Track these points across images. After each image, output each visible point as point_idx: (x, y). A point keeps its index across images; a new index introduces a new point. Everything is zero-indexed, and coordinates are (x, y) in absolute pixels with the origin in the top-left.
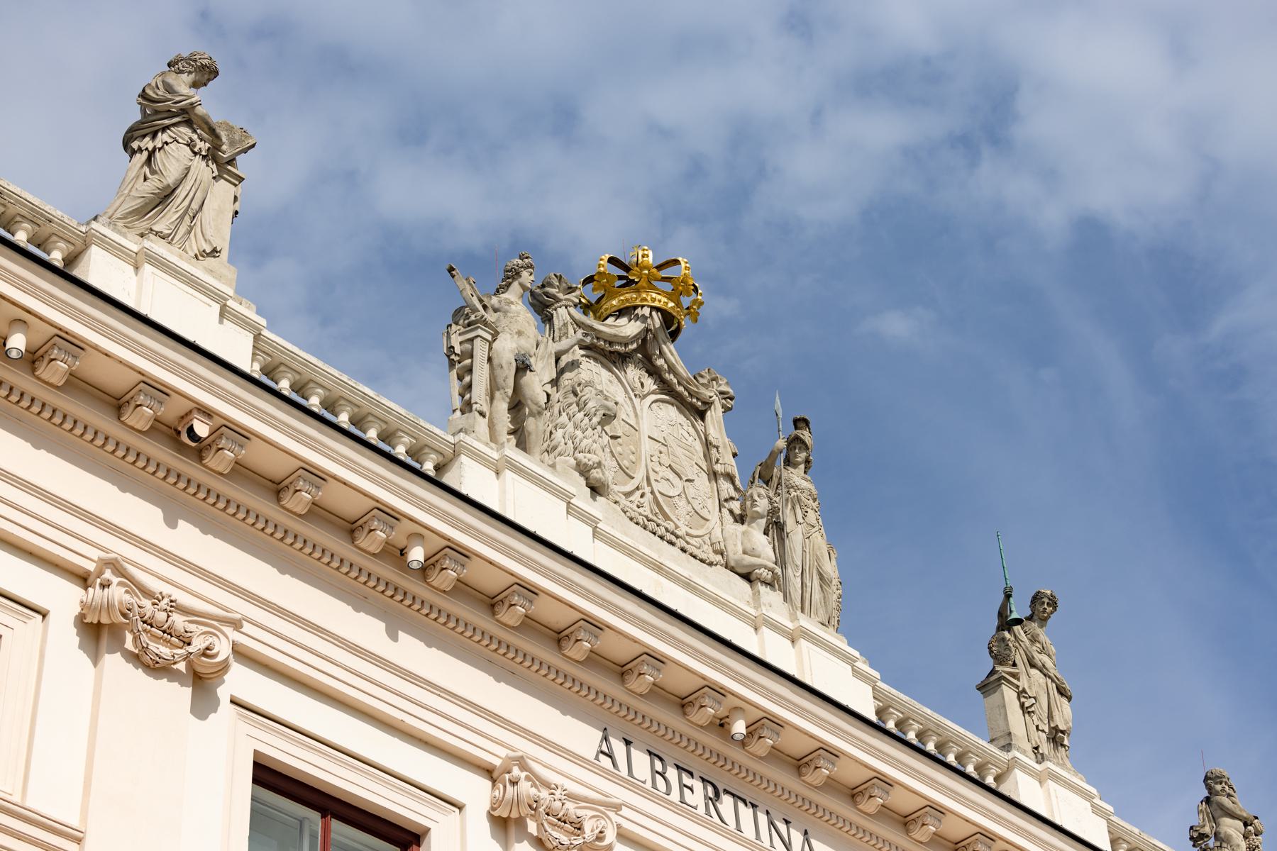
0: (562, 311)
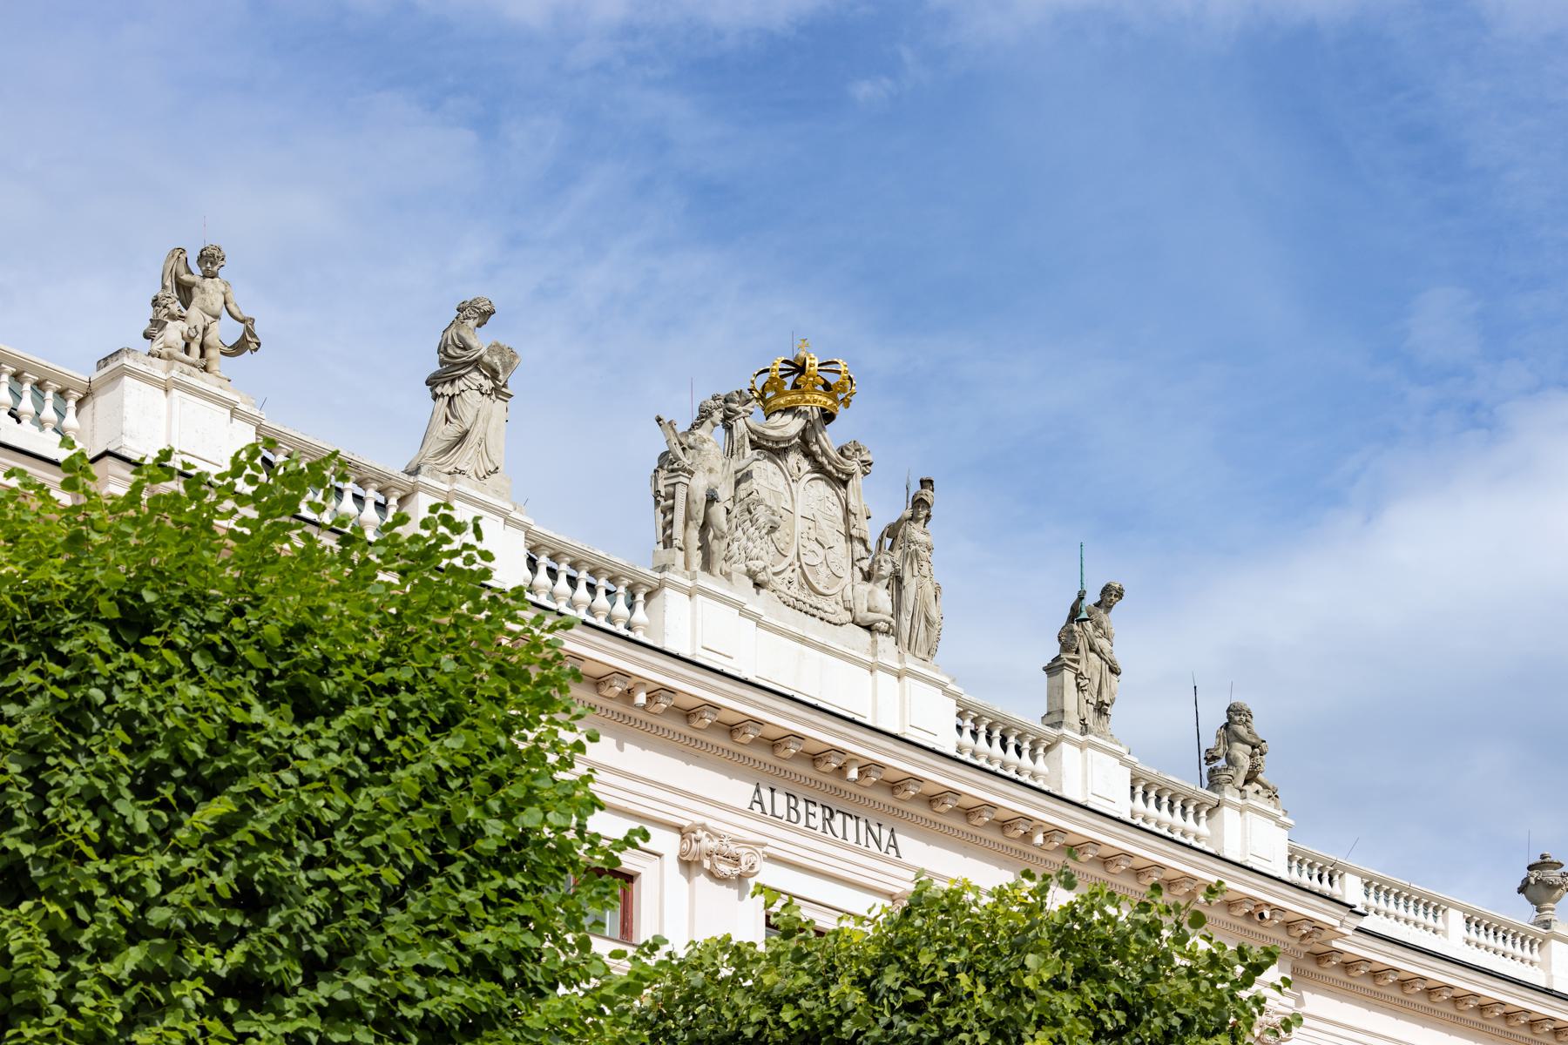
0: (740, 423)
